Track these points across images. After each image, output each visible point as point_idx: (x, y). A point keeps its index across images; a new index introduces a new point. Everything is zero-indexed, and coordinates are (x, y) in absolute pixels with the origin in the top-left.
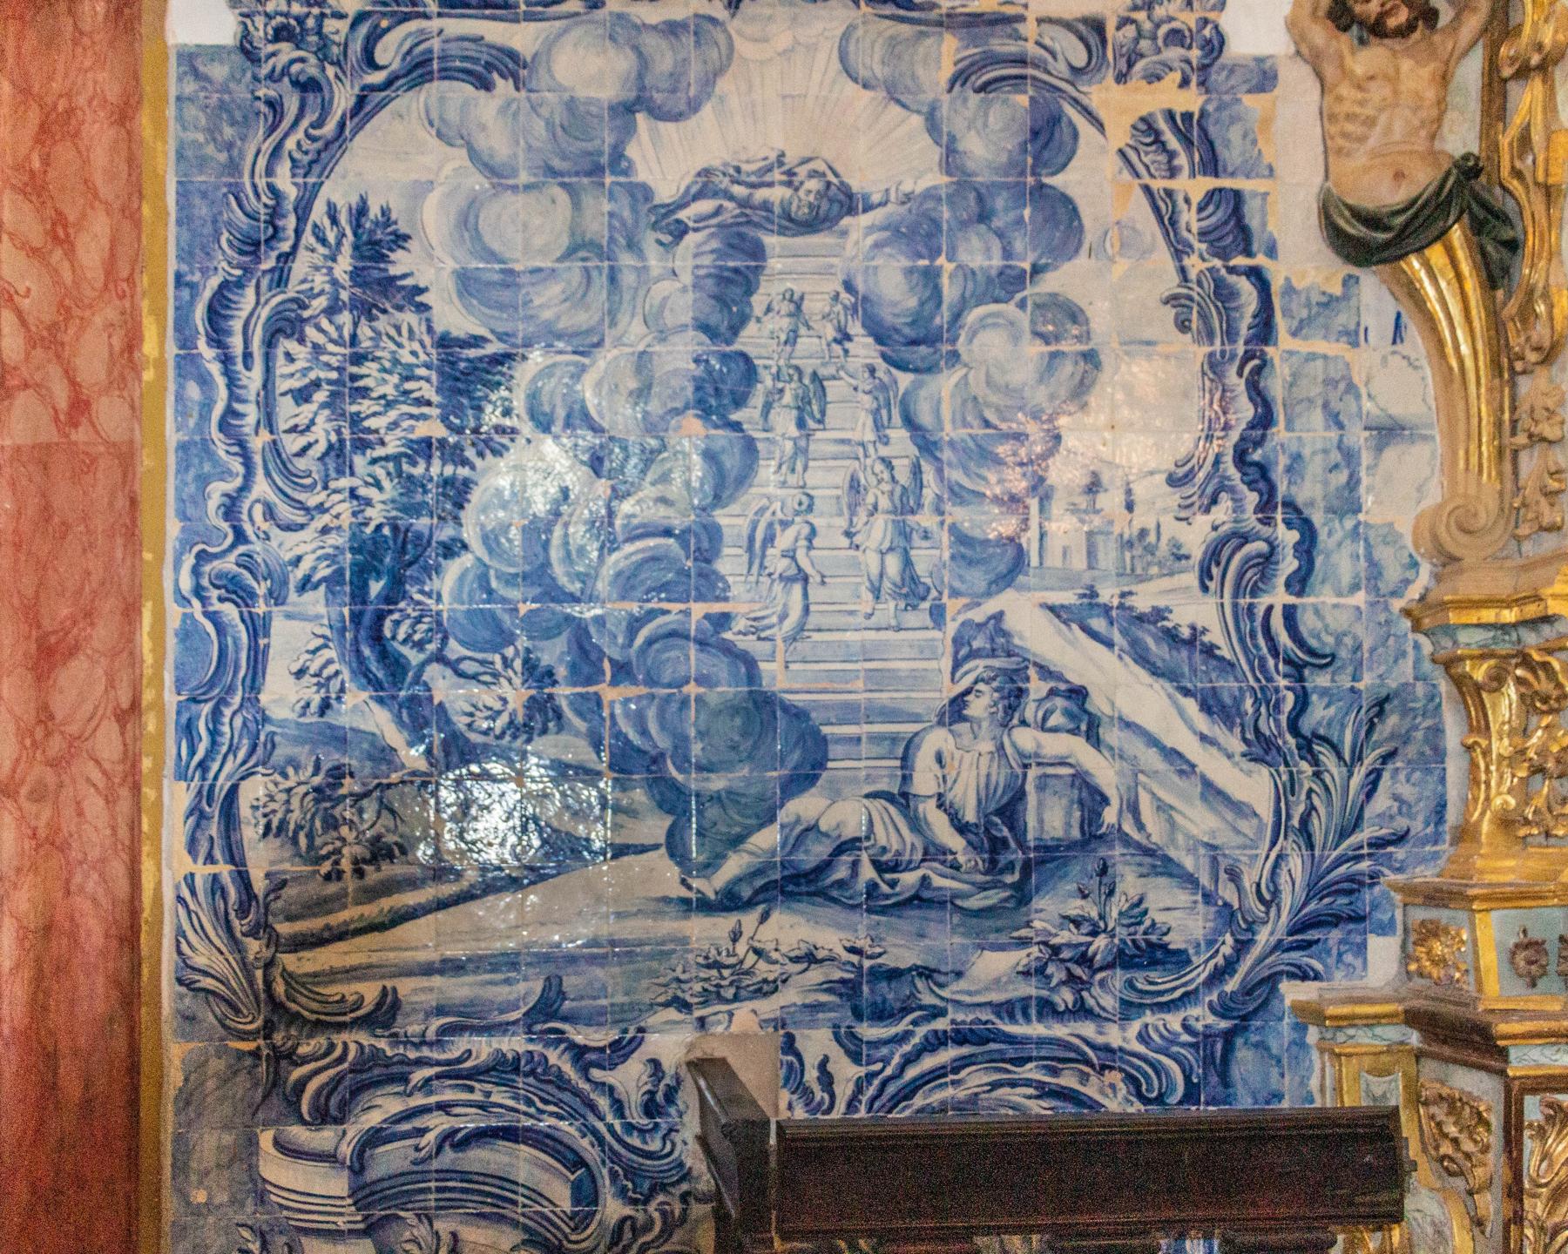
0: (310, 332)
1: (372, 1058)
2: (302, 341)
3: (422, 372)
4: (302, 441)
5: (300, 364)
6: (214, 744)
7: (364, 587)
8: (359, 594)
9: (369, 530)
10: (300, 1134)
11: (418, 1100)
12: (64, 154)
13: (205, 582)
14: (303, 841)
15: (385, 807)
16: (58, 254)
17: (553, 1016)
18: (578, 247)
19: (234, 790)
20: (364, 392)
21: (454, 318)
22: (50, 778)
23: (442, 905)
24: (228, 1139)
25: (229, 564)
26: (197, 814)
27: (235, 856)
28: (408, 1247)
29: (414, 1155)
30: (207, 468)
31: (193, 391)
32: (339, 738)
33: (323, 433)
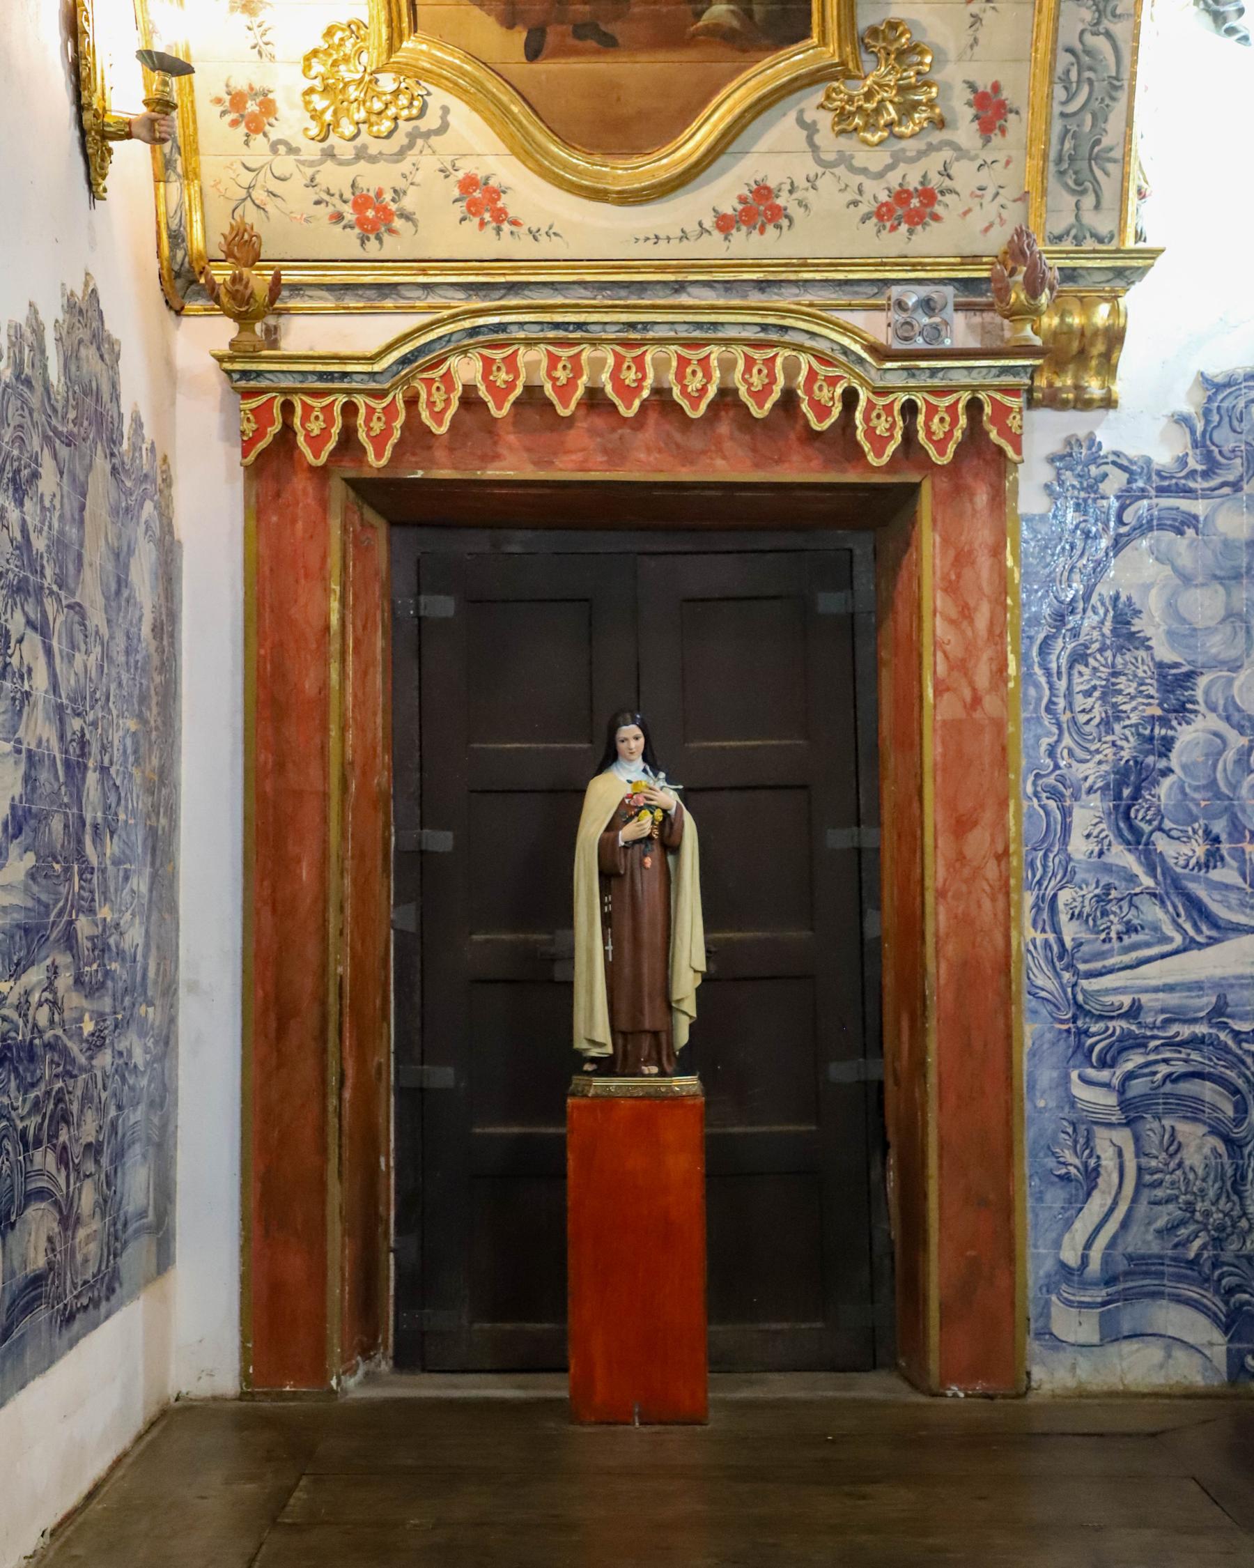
0: (1091, 661)
1: (1126, 1035)
2: (1087, 665)
3: (1148, 681)
4: (1087, 717)
5: (1086, 678)
6: (1045, 872)
7: (1120, 793)
8: (1118, 796)
9: (1123, 762)
10: (1091, 1073)
11: (1152, 1057)
12: (968, 573)
13: (1039, 789)
14: (1091, 922)
15: (1131, 904)
16: (965, 623)
17: (1222, 1015)
18: (1231, 615)
19: (1055, 896)
20: (1120, 692)
21: (1165, 653)
22: (964, 888)
23: (1163, 956)
24: (1055, 1074)
25: (1051, 780)
26: (1037, 907)
27: (1057, 930)
28: (1150, 1133)
29: (1151, 1085)
30: (1039, 731)
31: (1032, 692)
32: (1108, 869)
33: (1098, 713)
